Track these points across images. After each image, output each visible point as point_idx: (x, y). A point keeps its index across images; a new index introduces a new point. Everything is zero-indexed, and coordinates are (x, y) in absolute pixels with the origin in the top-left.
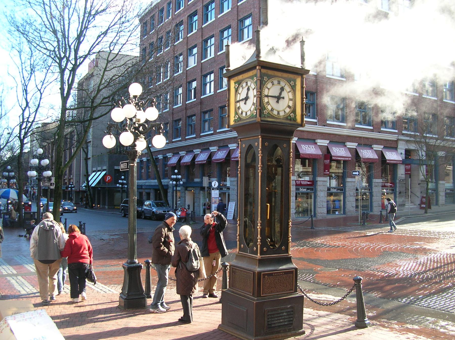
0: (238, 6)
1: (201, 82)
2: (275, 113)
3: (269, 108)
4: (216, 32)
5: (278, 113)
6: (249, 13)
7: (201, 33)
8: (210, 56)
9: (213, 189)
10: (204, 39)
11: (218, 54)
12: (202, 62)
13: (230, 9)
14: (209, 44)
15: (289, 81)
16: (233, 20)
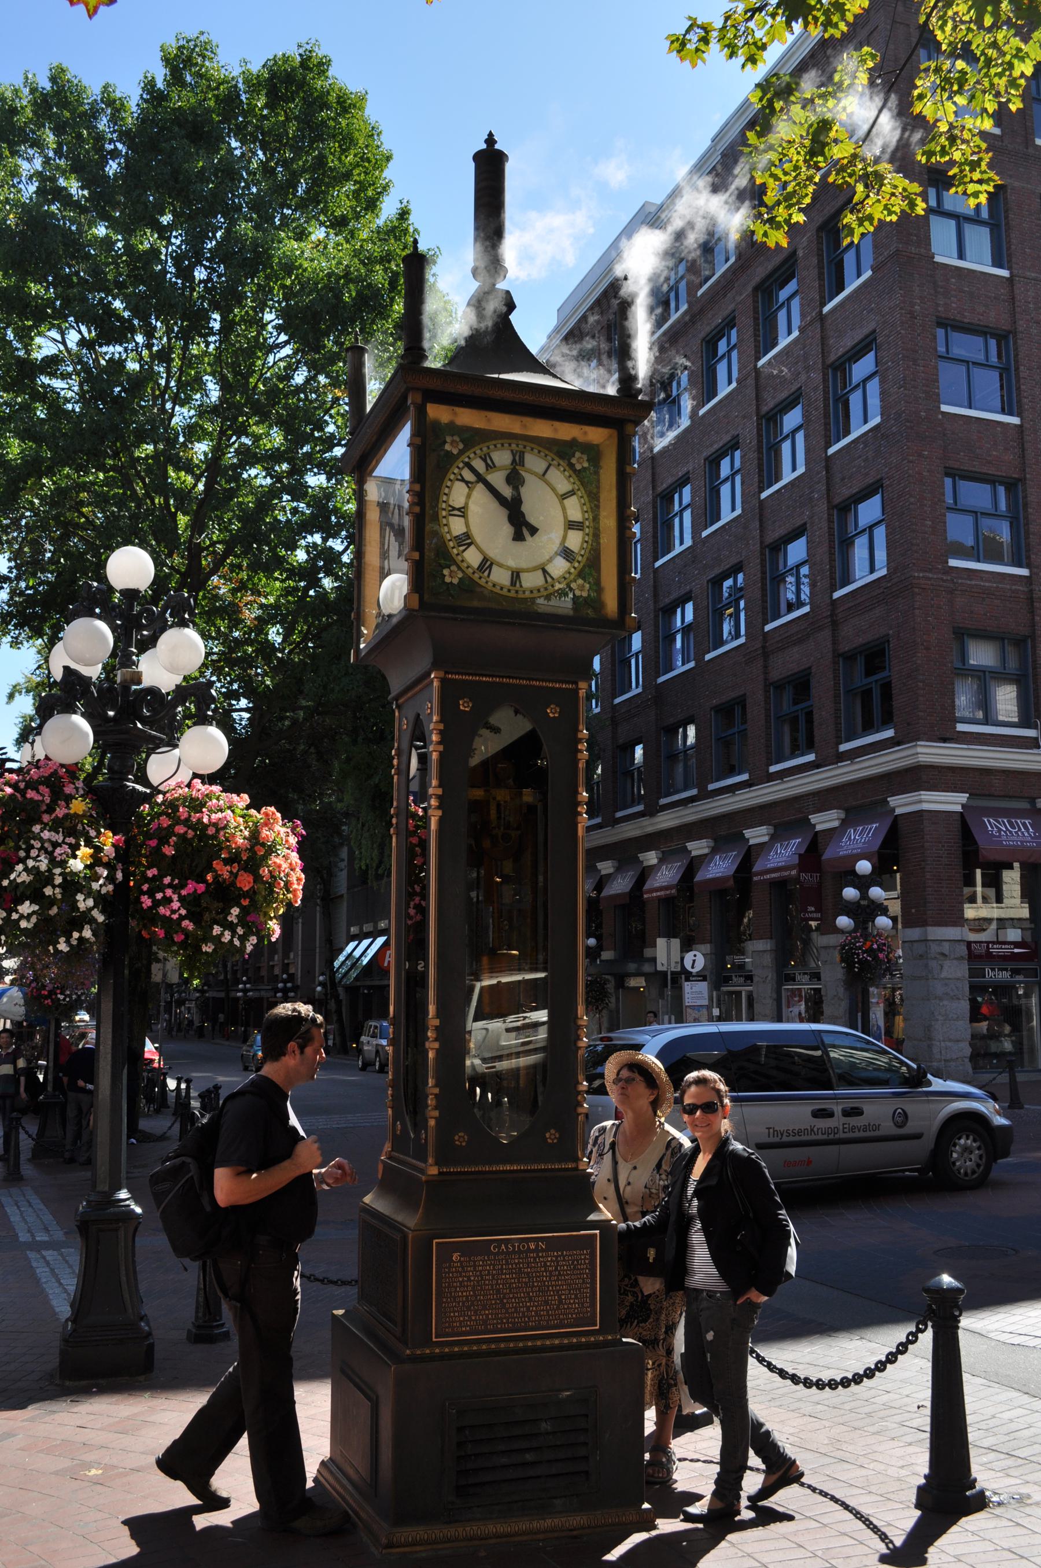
1: (657, 631)
2: (500, 577)
3: (472, 557)
4: (695, 464)
6: (794, 388)
8: (682, 543)
9: (687, 980)
10: (659, 490)
11: (704, 534)
12: (658, 564)
13: (734, 385)
14: (677, 508)
16: (744, 417)
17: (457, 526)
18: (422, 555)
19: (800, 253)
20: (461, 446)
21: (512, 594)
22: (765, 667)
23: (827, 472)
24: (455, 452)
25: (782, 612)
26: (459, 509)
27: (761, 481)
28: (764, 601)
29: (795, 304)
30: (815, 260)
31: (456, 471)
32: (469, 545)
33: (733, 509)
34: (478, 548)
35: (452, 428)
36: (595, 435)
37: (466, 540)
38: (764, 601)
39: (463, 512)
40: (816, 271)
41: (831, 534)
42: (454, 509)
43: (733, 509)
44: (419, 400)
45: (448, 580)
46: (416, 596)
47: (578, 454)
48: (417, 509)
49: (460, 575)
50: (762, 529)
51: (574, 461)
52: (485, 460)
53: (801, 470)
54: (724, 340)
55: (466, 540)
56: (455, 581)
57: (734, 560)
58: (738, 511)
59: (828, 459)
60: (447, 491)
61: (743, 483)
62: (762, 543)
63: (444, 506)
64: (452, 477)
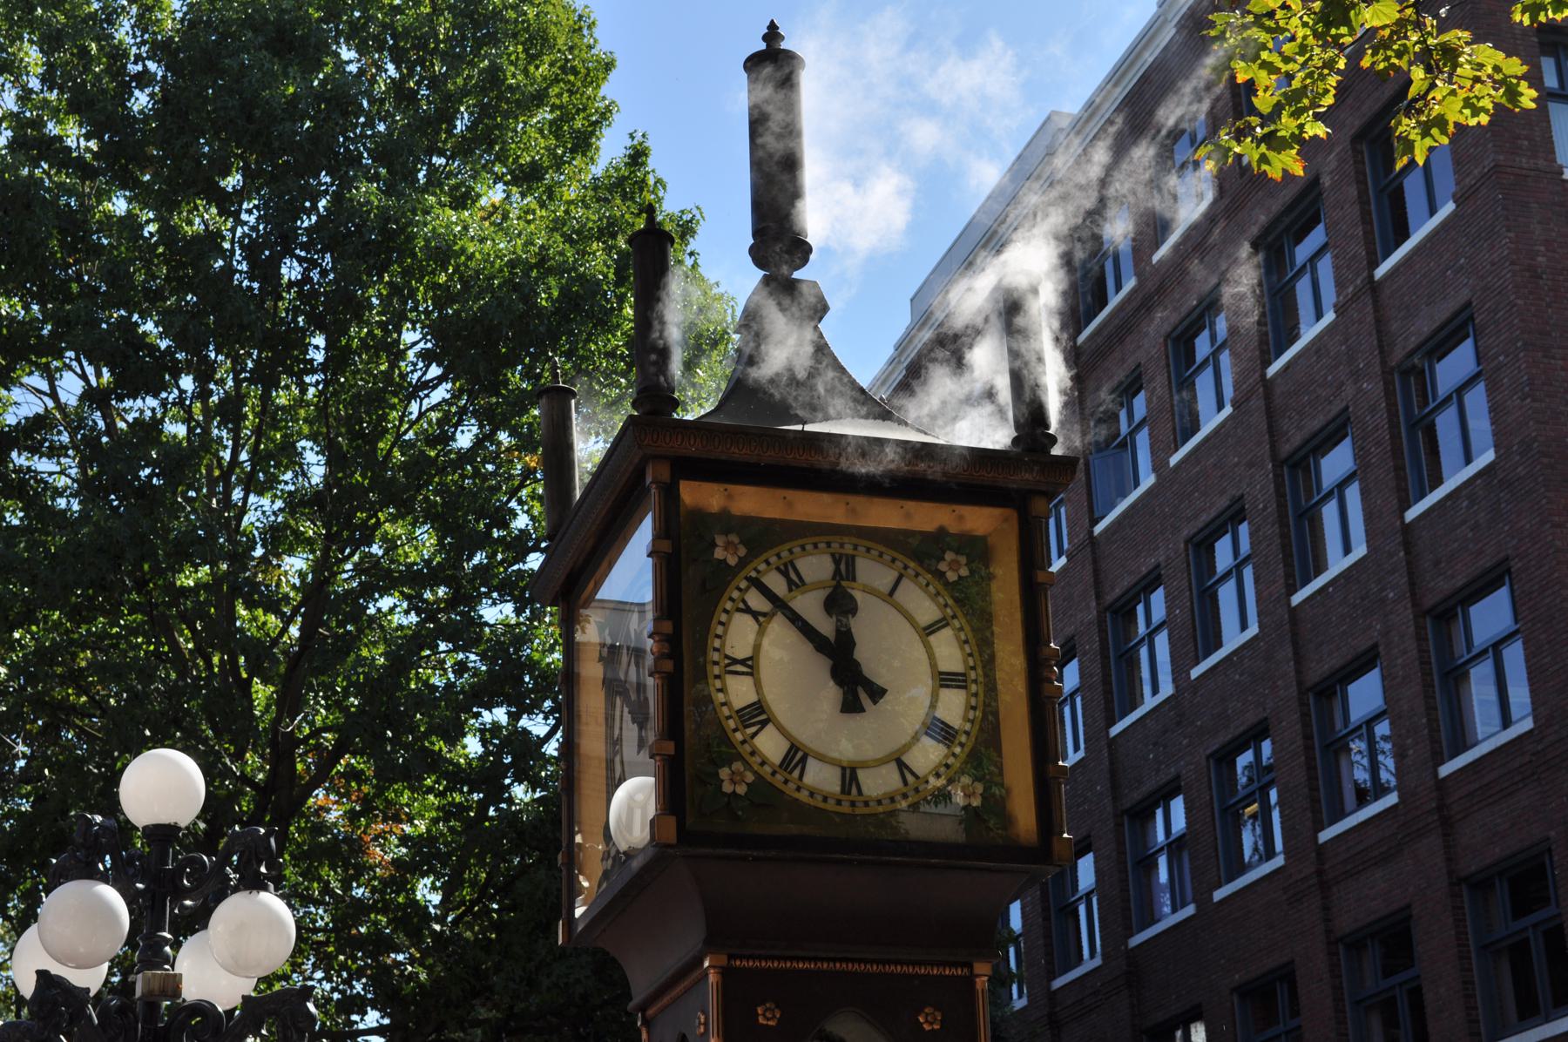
0: (1268, 385)
2: (820, 777)
3: (770, 745)
4: (1169, 550)
5: (849, 775)
6: (1335, 410)
7: (1089, 568)
8: (1155, 691)
10: (1110, 598)
11: (1195, 673)
12: (1115, 730)
14: (1142, 629)
15: (921, 552)
16: (1251, 465)
17: (740, 692)
18: (680, 747)
19: (1326, 181)
20: (742, 551)
21: (845, 808)
22: (1326, 908)
23: (1407, 553)
24: (732, 561)
25: (1348, 807)
26: (743, 662)
27: (1289, 575)
28: (1314, 789)
29: (1325, 267)
30: (1353, 192)
31: (736, 594)
32: (764, 724)
33: (1244, 626)
34: (781, 729)
35: (727, 522)
36: (978, 520)
37: (758, 714)
38: (1314, 789)
39: (750, 666)
40: (1356, 209)
41: (1424, 662)
42: (735, 661)
43: (1244, 626)
44: (665, 475)
45: (727, 788)
46: (672, 820)
47: (949, 556)
48: (668, 666)
49: (750, 777)
50: (1299, 659)
51: (943, 567)
52: (785, 574)
53: (1360, 551)
54: (1206, 333)
55: (758, 714)
56: (741, 790)
57: (1251, 718)
58: (1253, 630)
59: (1407, 529)
60: (720, 630)
61: (1257, 581)
62: (1300, 683)
63: (716, 656)
64: (729, 605)
